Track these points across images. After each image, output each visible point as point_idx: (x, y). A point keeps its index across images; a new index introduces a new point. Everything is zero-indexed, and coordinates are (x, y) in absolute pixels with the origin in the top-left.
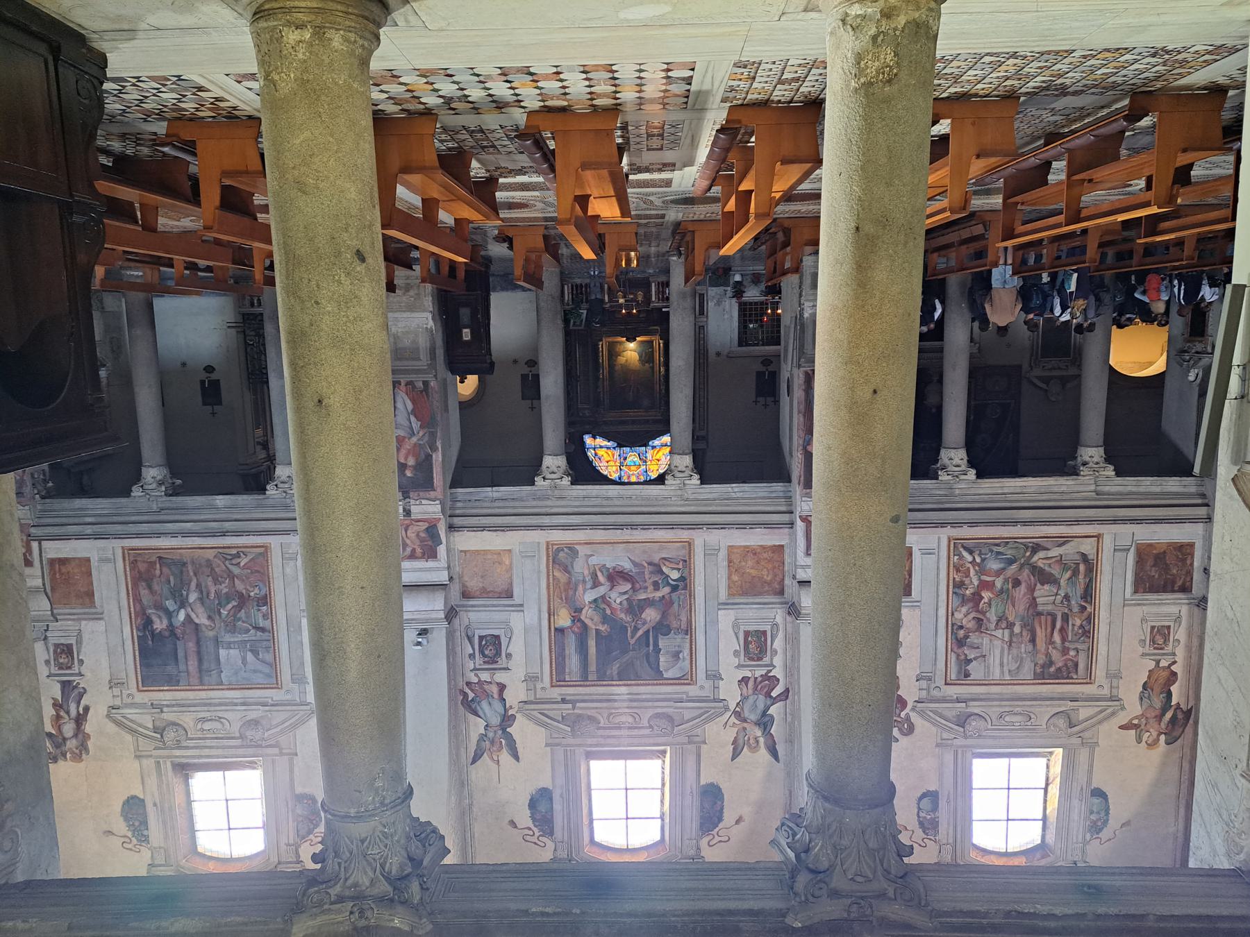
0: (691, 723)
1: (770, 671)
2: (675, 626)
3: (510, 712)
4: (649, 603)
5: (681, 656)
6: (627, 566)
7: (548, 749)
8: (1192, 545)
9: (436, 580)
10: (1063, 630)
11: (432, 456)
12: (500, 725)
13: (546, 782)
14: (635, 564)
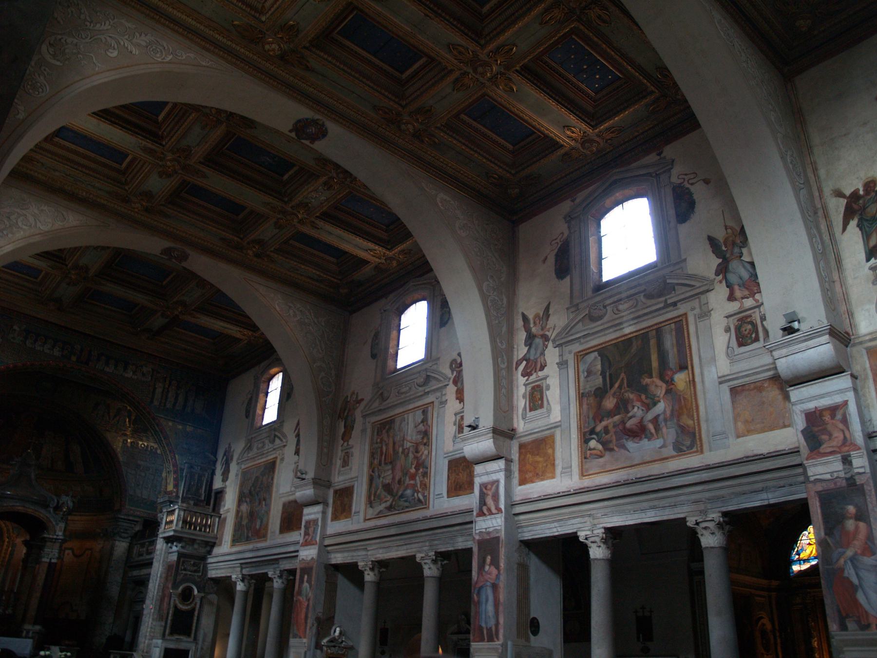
0: (577, 320)
1: (527, 380)
3: (721, 277)
4: (611, 414)
5: (586, 374)
6: (631, 445)
7: (683, 258)
8: (332, 520)
9: (802, 389)
11: (826, 534)
14: (624, 447)
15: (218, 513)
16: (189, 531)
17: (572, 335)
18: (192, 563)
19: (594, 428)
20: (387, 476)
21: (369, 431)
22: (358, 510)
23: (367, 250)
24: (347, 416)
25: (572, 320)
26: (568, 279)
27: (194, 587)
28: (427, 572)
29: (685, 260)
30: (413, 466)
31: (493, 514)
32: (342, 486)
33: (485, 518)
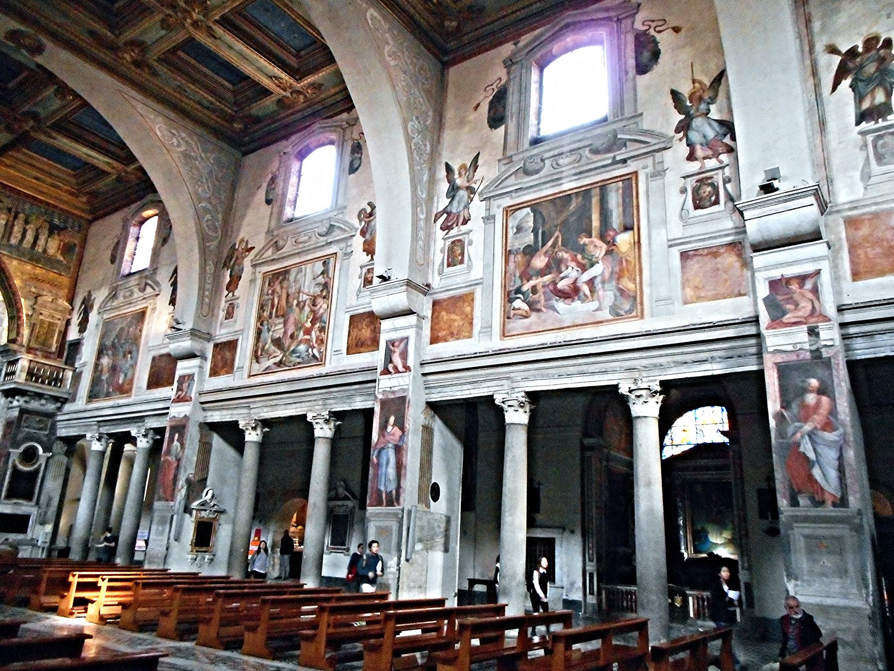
0: (509, 173)
2: (519, 256)
3: (681, 134)
4: (542, 273)
5: (515, 230)
6: (561, 305)
7: (639, 112)
8: (211, 375)
10: (273, 307)
11: (782, 407)
12: (692, 119)
13: (643, 80)
15: (72, 365)
16: (37, 385)
17: (502, 188)
18: (38, 419)
19: (521, 287)
20: (278, 330)
21: (259, 281)
22: (241, 365)
23: (271, 77)
24: (233, 265)
25: (504, 173)
26: (503, 127)
27: (39, 447)
28: (318, 433)
29: (641, 114)
30: (309, 320)
31: (399, 372)
32: (224, 340)
33: (389, 376)
